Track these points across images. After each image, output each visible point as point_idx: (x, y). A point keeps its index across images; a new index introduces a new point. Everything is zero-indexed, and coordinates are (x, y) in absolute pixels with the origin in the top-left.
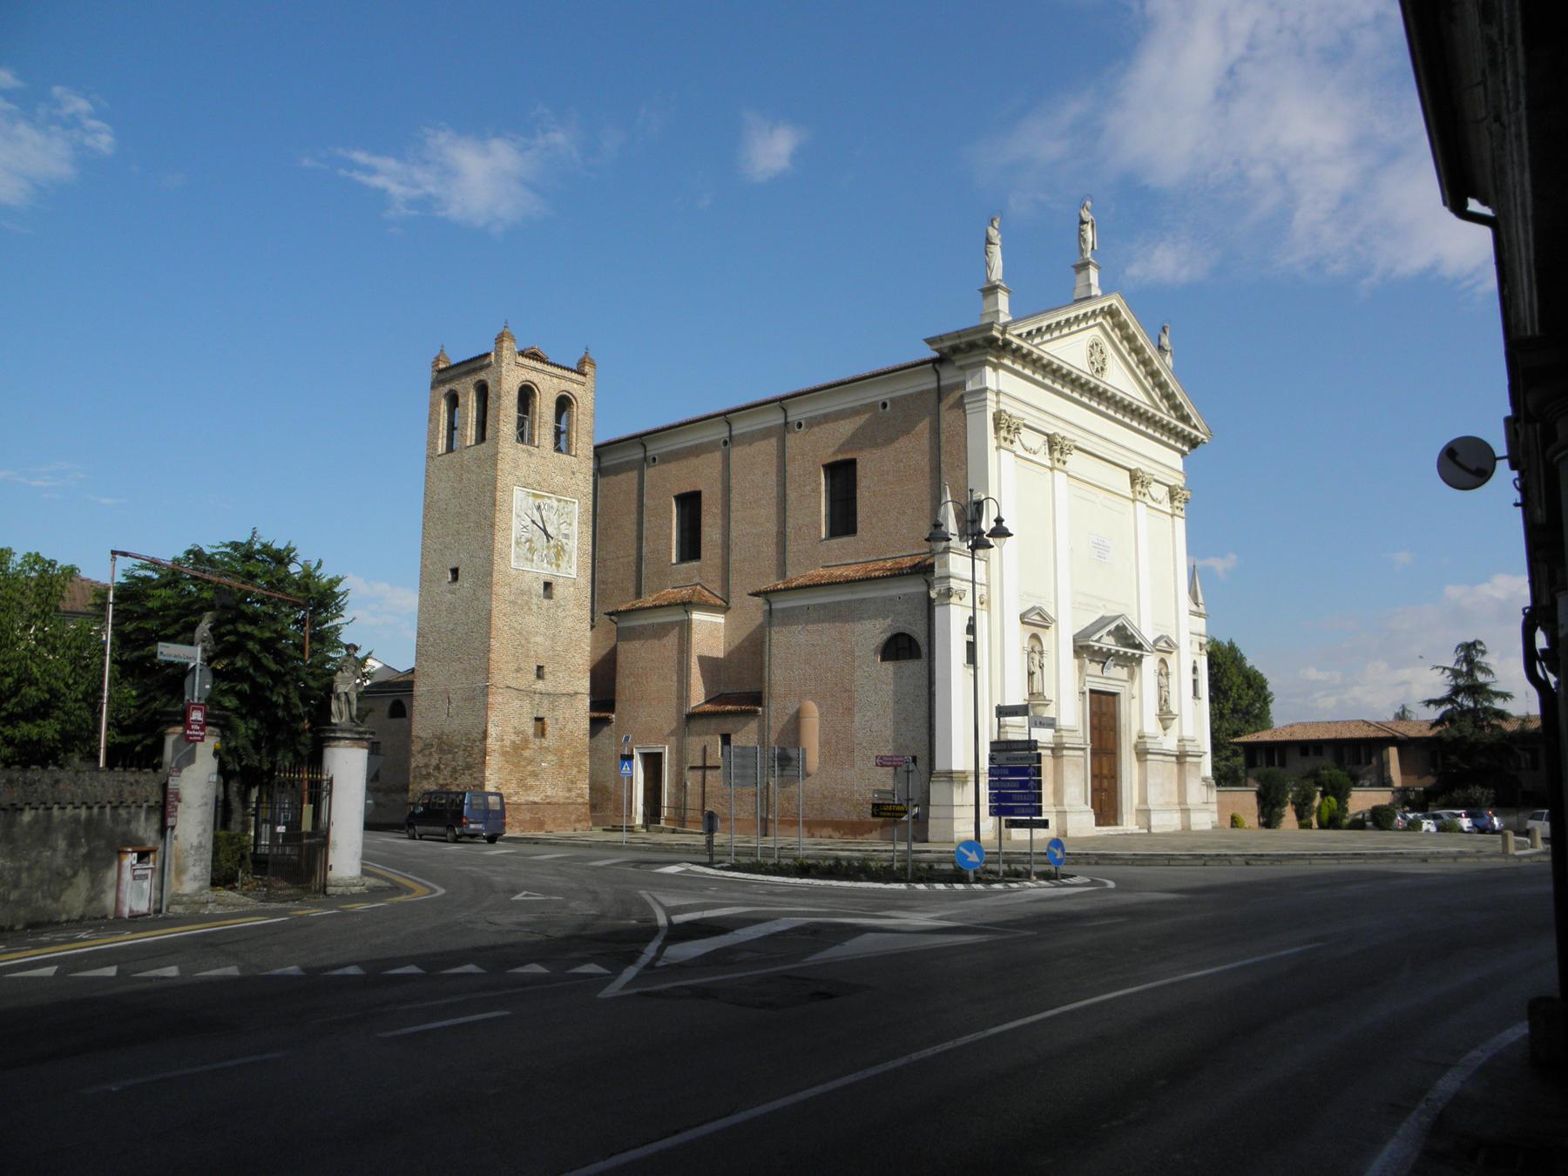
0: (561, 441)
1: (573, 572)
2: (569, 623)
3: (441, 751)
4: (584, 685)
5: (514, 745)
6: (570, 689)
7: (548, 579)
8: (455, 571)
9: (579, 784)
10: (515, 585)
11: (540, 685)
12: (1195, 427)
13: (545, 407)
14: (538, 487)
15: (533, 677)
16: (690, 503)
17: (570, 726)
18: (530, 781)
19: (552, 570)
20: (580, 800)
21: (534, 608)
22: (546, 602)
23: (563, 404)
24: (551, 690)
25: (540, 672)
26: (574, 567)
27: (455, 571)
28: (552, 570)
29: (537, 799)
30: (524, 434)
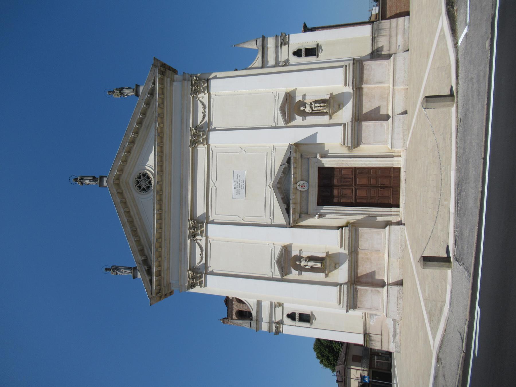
12: (154, 83)
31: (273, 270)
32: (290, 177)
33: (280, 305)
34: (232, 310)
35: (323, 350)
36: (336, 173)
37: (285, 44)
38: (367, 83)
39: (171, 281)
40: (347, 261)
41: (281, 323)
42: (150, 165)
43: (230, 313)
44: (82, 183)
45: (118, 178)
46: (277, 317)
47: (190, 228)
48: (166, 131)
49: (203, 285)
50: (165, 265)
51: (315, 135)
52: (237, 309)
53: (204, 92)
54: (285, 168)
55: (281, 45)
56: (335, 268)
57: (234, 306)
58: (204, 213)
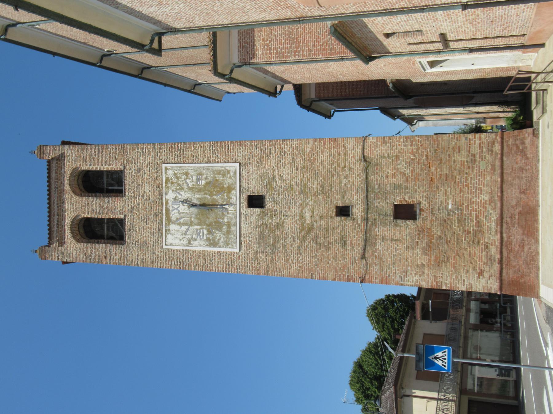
2: (286, 171)
5: (427, 250)
6: (359, 167)
7: (244, 202)
9: (475, 149)
10: (256, 247)
11: (357, 212)
14: (161, 217)
15: (349, 222)
17: (402, 166)
18: (472, 226)
20: (497, 147)
21: (276, 220)
22: (269, 204)
24: (362, 196)
25: (344, 211)
28: (235, 196)
29: (495, 216)
34: (61, 219)
35: (367, 384)
43: (54, 228)
52: (73, 215)
57: (67, 206)
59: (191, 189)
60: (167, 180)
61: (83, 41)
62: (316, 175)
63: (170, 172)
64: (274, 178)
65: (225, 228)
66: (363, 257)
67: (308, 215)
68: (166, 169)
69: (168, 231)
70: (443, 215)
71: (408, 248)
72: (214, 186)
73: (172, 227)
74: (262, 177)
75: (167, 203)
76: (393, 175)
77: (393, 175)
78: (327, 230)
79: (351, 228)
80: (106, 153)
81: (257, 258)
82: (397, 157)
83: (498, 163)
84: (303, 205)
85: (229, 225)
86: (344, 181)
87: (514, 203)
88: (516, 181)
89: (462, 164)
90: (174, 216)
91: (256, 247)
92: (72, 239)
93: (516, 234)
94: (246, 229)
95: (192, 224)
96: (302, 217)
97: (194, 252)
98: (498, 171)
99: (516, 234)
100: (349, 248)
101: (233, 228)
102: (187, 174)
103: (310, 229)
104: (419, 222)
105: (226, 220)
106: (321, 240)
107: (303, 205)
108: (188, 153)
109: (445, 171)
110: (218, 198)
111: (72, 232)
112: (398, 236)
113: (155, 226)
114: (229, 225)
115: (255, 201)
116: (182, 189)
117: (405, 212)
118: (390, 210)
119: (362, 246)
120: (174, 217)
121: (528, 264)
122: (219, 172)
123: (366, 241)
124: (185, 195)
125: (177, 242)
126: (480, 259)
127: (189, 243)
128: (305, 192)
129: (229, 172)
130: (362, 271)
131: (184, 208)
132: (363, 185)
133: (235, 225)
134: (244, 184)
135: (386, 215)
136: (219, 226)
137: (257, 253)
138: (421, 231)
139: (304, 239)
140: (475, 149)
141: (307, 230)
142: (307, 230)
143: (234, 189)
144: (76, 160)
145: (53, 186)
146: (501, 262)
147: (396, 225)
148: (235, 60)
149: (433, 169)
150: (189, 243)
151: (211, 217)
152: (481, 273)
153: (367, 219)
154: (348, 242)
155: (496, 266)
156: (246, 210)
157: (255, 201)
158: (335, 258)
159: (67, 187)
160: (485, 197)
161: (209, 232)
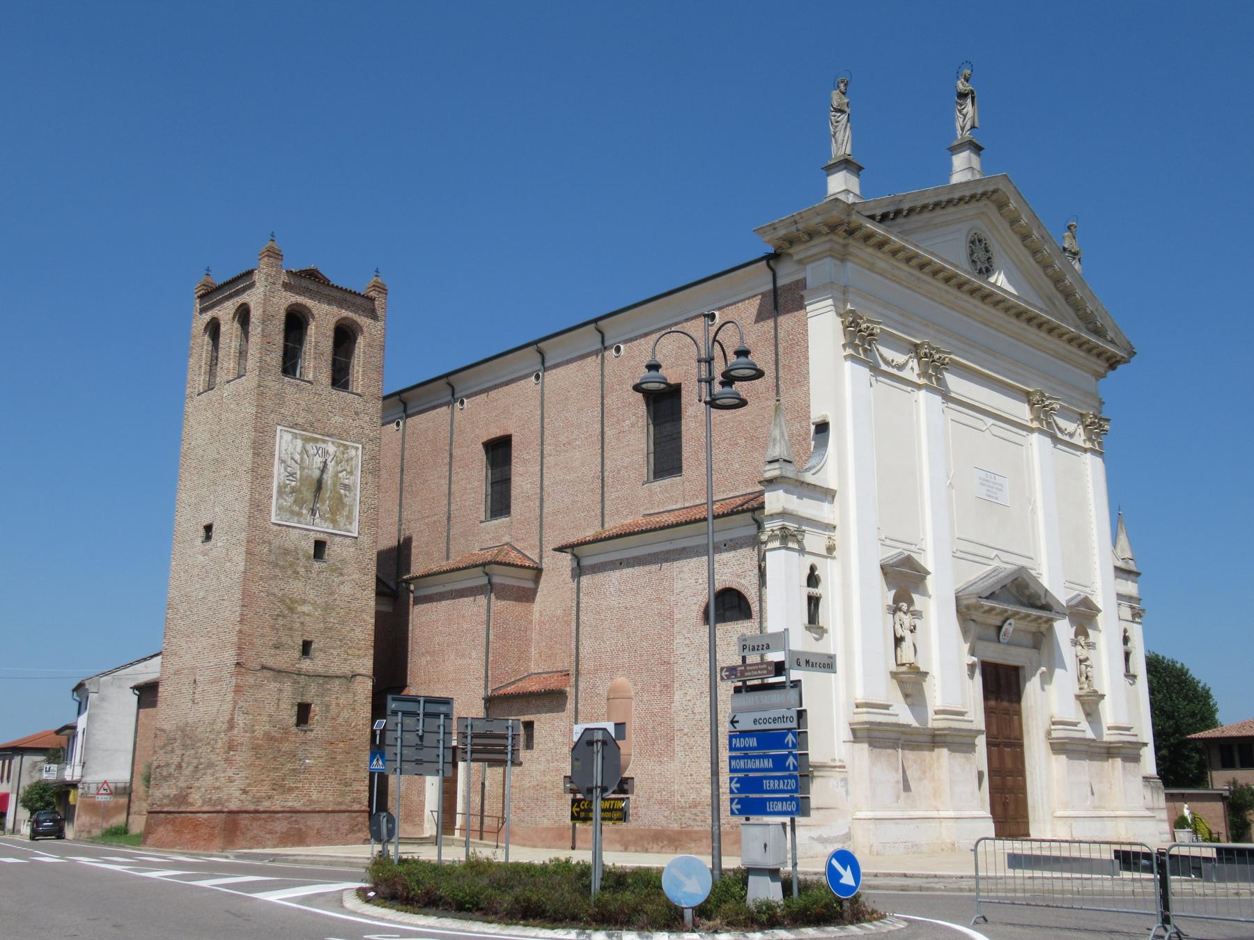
0: (340, 378)
1: (354, 530)
2: (346, 589)
3: (185, 747)
4: (365, 664)
5: (269, 738)
6: (346, 669)
7: (321, 537)
8: (208, 528)
9: (356, 786)
10: (276, 542)
11: (306, 665)
12: (1112, 342)
13: (319, 337)
14: (312, 430)
15: (297, 654)
16: (499, 450)
17: (345, 714)
18: (289, 783)
19: (327, 527)
20: (356, 807)
21: (302, 570)
22: (317, 565)
23: (344, 337)
24: (321, 670)
25: (306, 648)
26: (356, 524)
27: (208, 528)
28: (327, 527)
29: (298, 805)
30: (290, 364)
31: (888, 542)
32: (1008, 602)
33: (830, 549)
36: (1015, 705)
37: (1133, 615)
38: (1124, 768)
39: (849, 265)
40: (915, 724)
41: (802, 551)
42: (999, 279)
44: (963, 96)
45: (1002, 206)
46: (814, 541)
47: (938, 351)
48: (1052, 342)
49: (849, 351)
50: (882, 261)
51: (1063, 667)
52: (315, 312)
53: (1090, 439)
54: (1039, 598)
55: (1132, 608)
56: (906, 696)
57: (325, 307)
58: (949, 391)
59: (336, 474)
60: (346, 447)
61: (493, 394)
62: (342, 623)
63: (353, 452)
64: (342, 574)
65: (296, 509)
66: (264, 668)
67: (306, 608)
68: (357, 449)
69: (295, 436)
70: (300, 754)
71: (271, 716)
72: (339, 504)
73: (299, 443)
74: (343, 561)
75: (324, 442)
76: (338, 705)
77: (338, 705)
78: (291, 629)
79: (289, 658)
80: (375, 376)
81: (264, 542)
82: (354, 709)
83: (343, 807)
84: (314, 604)
85: (299, 514)
86: (335, 653)
87: (309, 823)
88: (327, 825)
89: (345, 774)
90: (311, 448)
91: (276, 542)
92: (289, 302)
93: (281, 826)
94: (294, 534)
95: (302, 468)
96: (304, 602)
97: (272, 465)
98: (338, 808)
99: (281, 826)
100: (273, 652)
101: (296, 519)
102: (351, 473)
103: (292, 610)
104: (294, 729)
105: (304, 511)
106: (281, 621)
107: (314, 604)
108: (370, 478)
109: (339, 757)
110: (325, 507)
111: (297, 304)
112: (283, 706)
113: (300, 421)
114: (299, 514)
115: (320, 546)
116: (338, 463)
117: (303, 713)
118: (307, 699)
119: (274, 666)
120: (309, 447)
121: (253, 838)
122: (351, 512)
123: (279, 671)
124: (331, 465)
125: (284, 446)
126: (258, 791)
127: (283, 462)
128: (327, 608)
129: (350, 524)
130: (249, 665)
131: (318, 461)
132: (330, 673)
133: (299, 522)
134: (338, 539)
135: (303, 695)
136: (299, 502)
137: (270, 543)
138: (286, 731)
139: (282, 601)
140: (356, 786)
141: (290, 605)
142: (290, 605)
143: (334, 528)
144: (370, 332)
145: (348, 297)
146: (256, 812)
147: (292, 705)
148: (496, 580)
149: (341, 745)
150: (283, 462)
151: (308, 495)
152: (245, 792)
153: (299, 675)
154: (278, 652)
155: (252, 807)
156: (313, 537)
157: (320, 546)
158: (262, 636)
159: (345, 313)
160: (315, 796)
161: (293, 491)
